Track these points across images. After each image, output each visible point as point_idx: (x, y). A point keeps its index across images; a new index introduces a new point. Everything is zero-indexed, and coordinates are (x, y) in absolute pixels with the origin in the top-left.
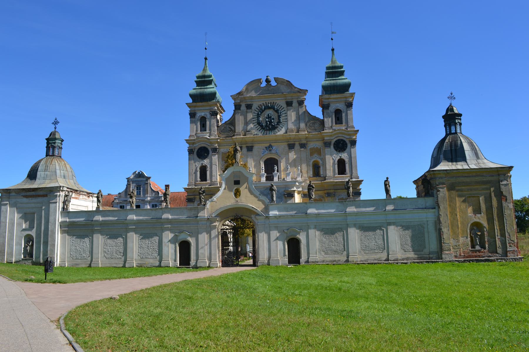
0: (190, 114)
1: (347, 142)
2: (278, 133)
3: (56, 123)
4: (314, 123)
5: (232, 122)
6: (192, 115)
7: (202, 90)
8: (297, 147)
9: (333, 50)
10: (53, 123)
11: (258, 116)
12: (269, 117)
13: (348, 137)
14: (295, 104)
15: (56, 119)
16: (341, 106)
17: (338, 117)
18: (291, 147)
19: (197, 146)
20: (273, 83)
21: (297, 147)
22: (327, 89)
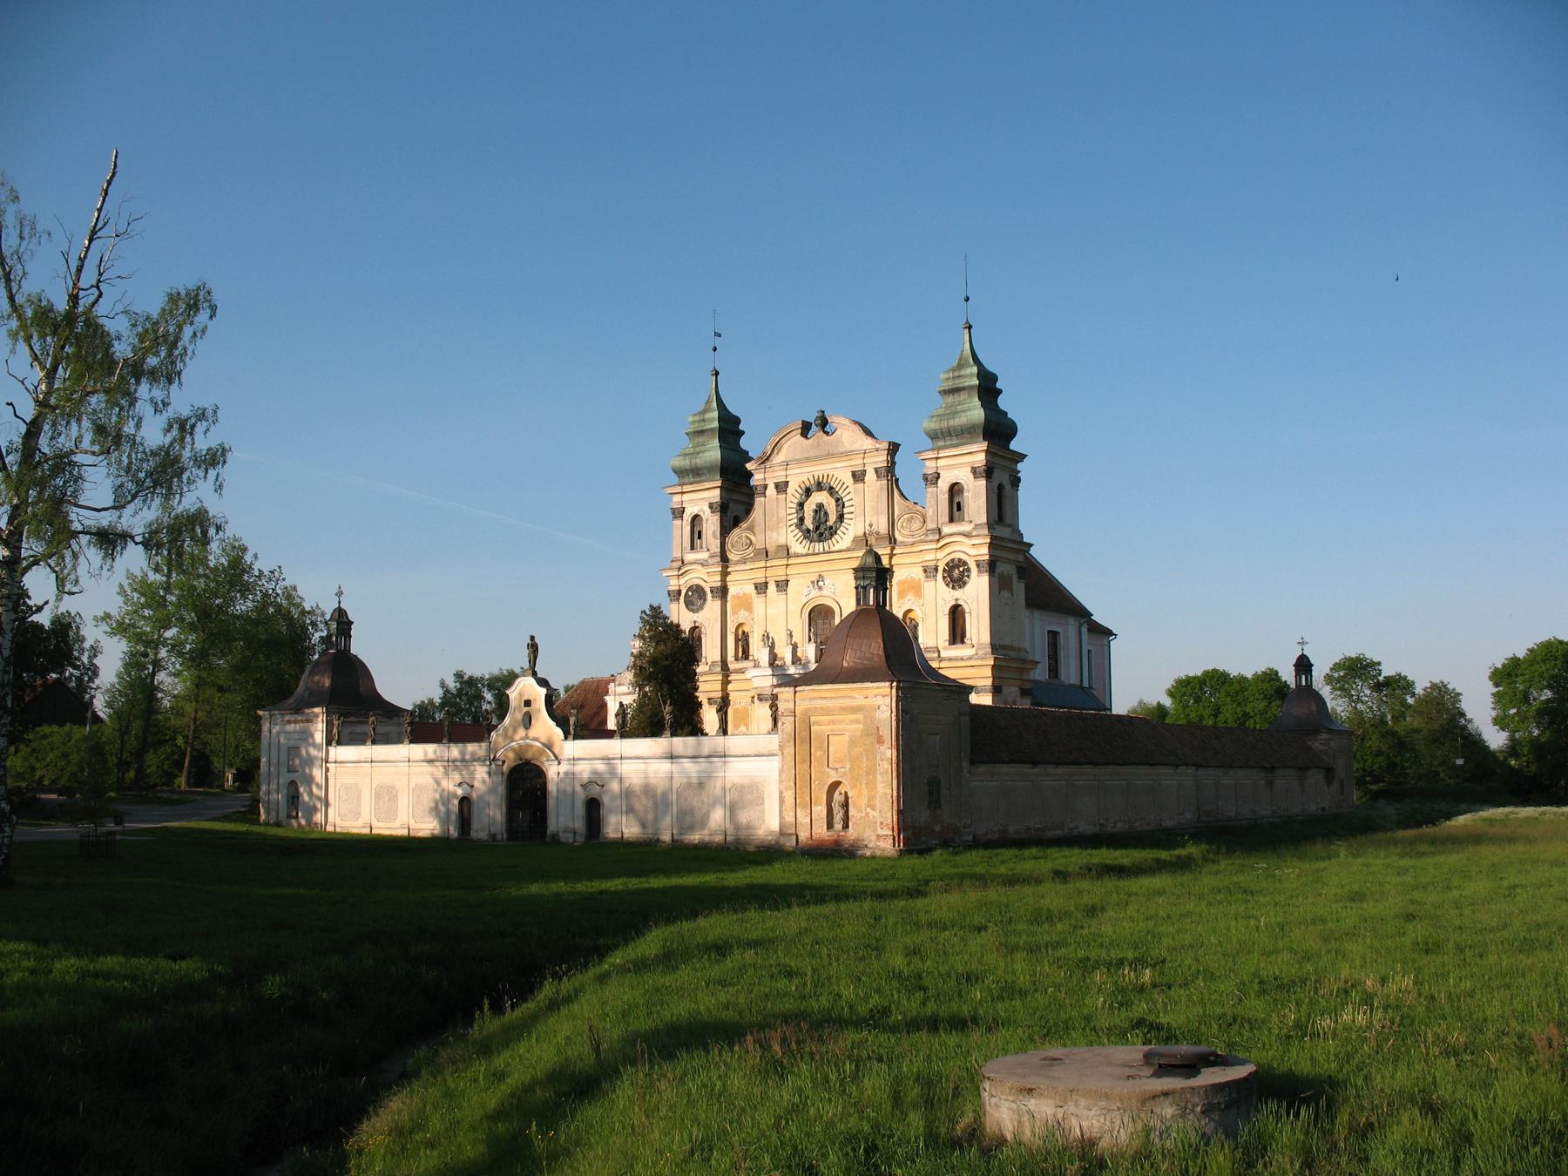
2: (837, 547)
12: (820, 507)
14: (871, 476)
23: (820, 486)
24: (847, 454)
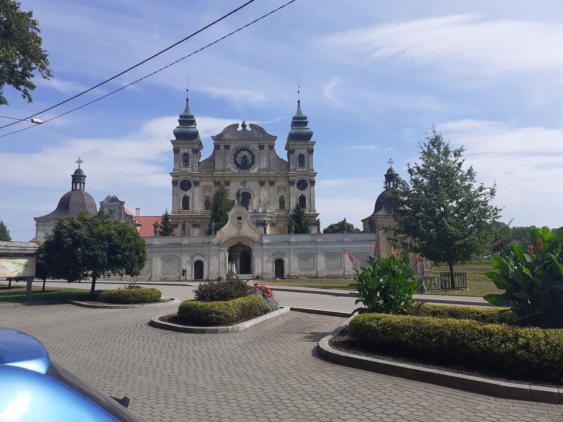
0: (174, 150)
1: (308, 182)
2: (252, 172)
3: (80, 162)
4: (281, 165)
5: (212, 159)
6: (176, 151)
7: (185, 129)
8: (267, 184)
9: (299, 102)
10: (77, 162)
11: (235, 156)
12: (245, 157)
13: (308, 178)
14: (266, 147)
15: (80, 159)
16: (304, 152)
17: (302, 160)
18: (262, 184)
19: (181, 179)
20: (248, 128)
21: (267, 184)
22: (292, 137)
23: (244, 149)
24: (258, 140)
